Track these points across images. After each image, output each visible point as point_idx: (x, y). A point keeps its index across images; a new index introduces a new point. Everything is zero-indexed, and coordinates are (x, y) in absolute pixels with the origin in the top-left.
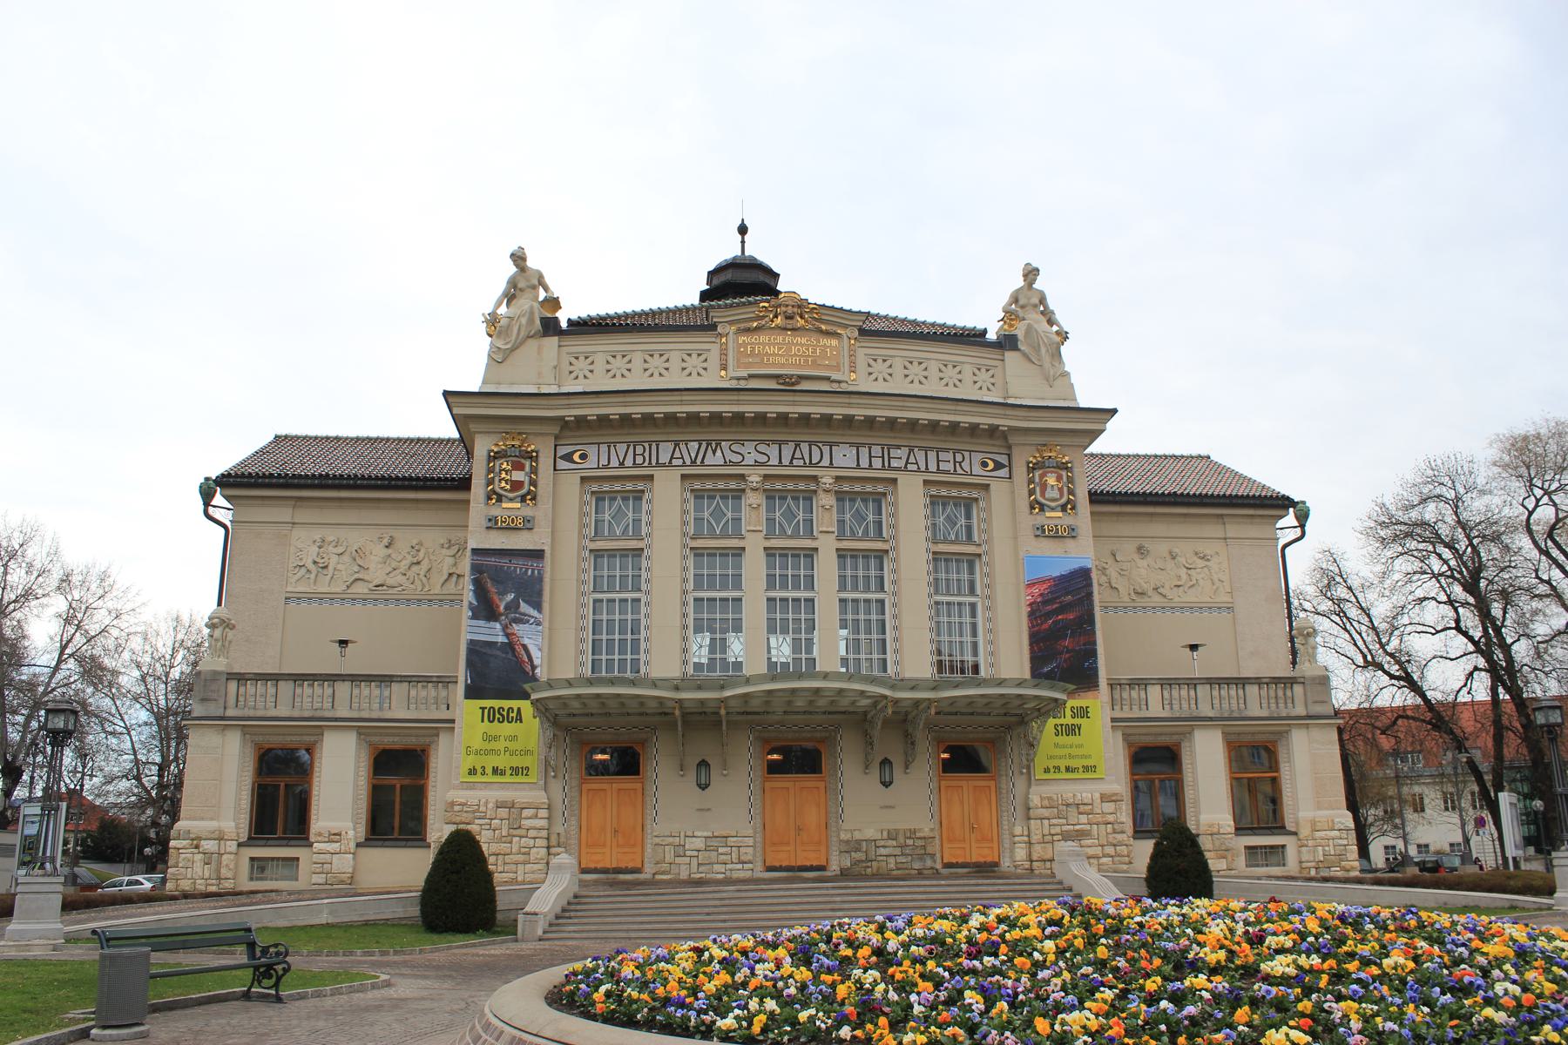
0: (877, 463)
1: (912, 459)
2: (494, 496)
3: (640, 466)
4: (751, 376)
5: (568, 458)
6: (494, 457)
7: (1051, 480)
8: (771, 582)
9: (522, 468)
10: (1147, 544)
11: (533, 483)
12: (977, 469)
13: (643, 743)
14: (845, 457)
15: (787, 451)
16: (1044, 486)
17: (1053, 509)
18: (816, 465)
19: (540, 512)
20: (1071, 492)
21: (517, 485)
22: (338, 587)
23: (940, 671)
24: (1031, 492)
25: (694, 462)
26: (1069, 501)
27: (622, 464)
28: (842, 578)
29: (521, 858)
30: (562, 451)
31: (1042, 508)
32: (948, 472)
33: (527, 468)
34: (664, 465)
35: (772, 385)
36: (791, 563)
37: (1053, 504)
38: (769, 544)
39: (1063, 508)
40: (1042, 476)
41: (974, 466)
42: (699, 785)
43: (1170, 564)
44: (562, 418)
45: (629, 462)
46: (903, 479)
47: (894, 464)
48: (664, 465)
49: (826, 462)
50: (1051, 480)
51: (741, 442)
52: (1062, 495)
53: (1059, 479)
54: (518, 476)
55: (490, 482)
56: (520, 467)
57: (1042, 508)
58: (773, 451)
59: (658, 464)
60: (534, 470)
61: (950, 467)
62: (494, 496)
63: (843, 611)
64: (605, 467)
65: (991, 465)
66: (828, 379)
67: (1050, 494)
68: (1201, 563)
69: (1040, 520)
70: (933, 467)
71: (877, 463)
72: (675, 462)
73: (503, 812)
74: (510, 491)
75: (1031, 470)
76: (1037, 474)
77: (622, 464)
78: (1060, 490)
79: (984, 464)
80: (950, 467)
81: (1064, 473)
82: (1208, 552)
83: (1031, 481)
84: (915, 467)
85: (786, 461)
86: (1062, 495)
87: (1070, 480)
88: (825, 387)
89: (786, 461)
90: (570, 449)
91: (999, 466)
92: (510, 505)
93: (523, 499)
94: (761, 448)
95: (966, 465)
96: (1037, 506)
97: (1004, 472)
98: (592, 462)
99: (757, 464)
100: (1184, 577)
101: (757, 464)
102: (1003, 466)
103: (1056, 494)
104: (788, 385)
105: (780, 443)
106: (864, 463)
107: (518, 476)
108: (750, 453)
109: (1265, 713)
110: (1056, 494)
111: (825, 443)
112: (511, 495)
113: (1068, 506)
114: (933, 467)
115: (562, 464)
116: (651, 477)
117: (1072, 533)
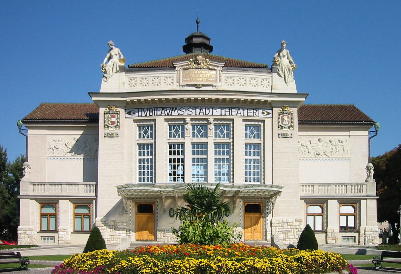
0: (227, 114)
1: (239, 112)
3: (152, 116)
4: (187, 85)
6: (106, 113)
8: (193, 153)
9: (114, 117)
10: (321, 138)
12: (261, 115)
13: (154, 203)
14: (217, 112)
15: (198, 111)
21: (113, 123)
22: (62, 155)
23: (246, 181)
24: (278, 123)
25: (168, 115)
27: (146, 115)
28: (216, 152)
31: (282, 127)
32: (250, 116)
33: (116, 117)
34: (159, 115)
36: (200, 148)
38: (192, 141)
39: (289, 128)
40: (282, 117)
41: (259, 114)
42: (170, 216)
43: (330, 144)
44: (126, 101)
45: (148, 115)
48: (159, 115)
49: (211, 113)
50: (286, 118)
52: (289, 123)
53: (288, 118)
54: (113, 120)
56: (114, 117)
57: (282, 127)
58: (194, 111)
61: (252, 114)
63: (216, 162)
64: (141, 116)
65: (266, 113)
66: (212, 86)
67: (285, 123)
68: (340, 144)
70: (246, 115)
71: (227, 114)
74: (112, 125)
75: (279, 115)
76: (281, 116)
77: (146, 115)
78: (288, 121)
79: (263, 113)
80: (252, 114)
81: (290, 116)
82: (343, 140)
83: (279, 118)
84: (240, 115)
85: (198, 114)
86: (289, 123)
88: (210, 88)
89: (198, 114)
90: (130, 110)
92: (112, 129)
93: (115, 127)
95: (257, 113)
97: (270, 115)
100: (334, 149)
102: (270, 113)
103: (287, 123)
106: (223, 113)
107: (113, 120)
108: (187, 112)
110: (287, 123)
112: (112, 126)
113: (291, 127)
114: (246, 115)
116: (154, 120)
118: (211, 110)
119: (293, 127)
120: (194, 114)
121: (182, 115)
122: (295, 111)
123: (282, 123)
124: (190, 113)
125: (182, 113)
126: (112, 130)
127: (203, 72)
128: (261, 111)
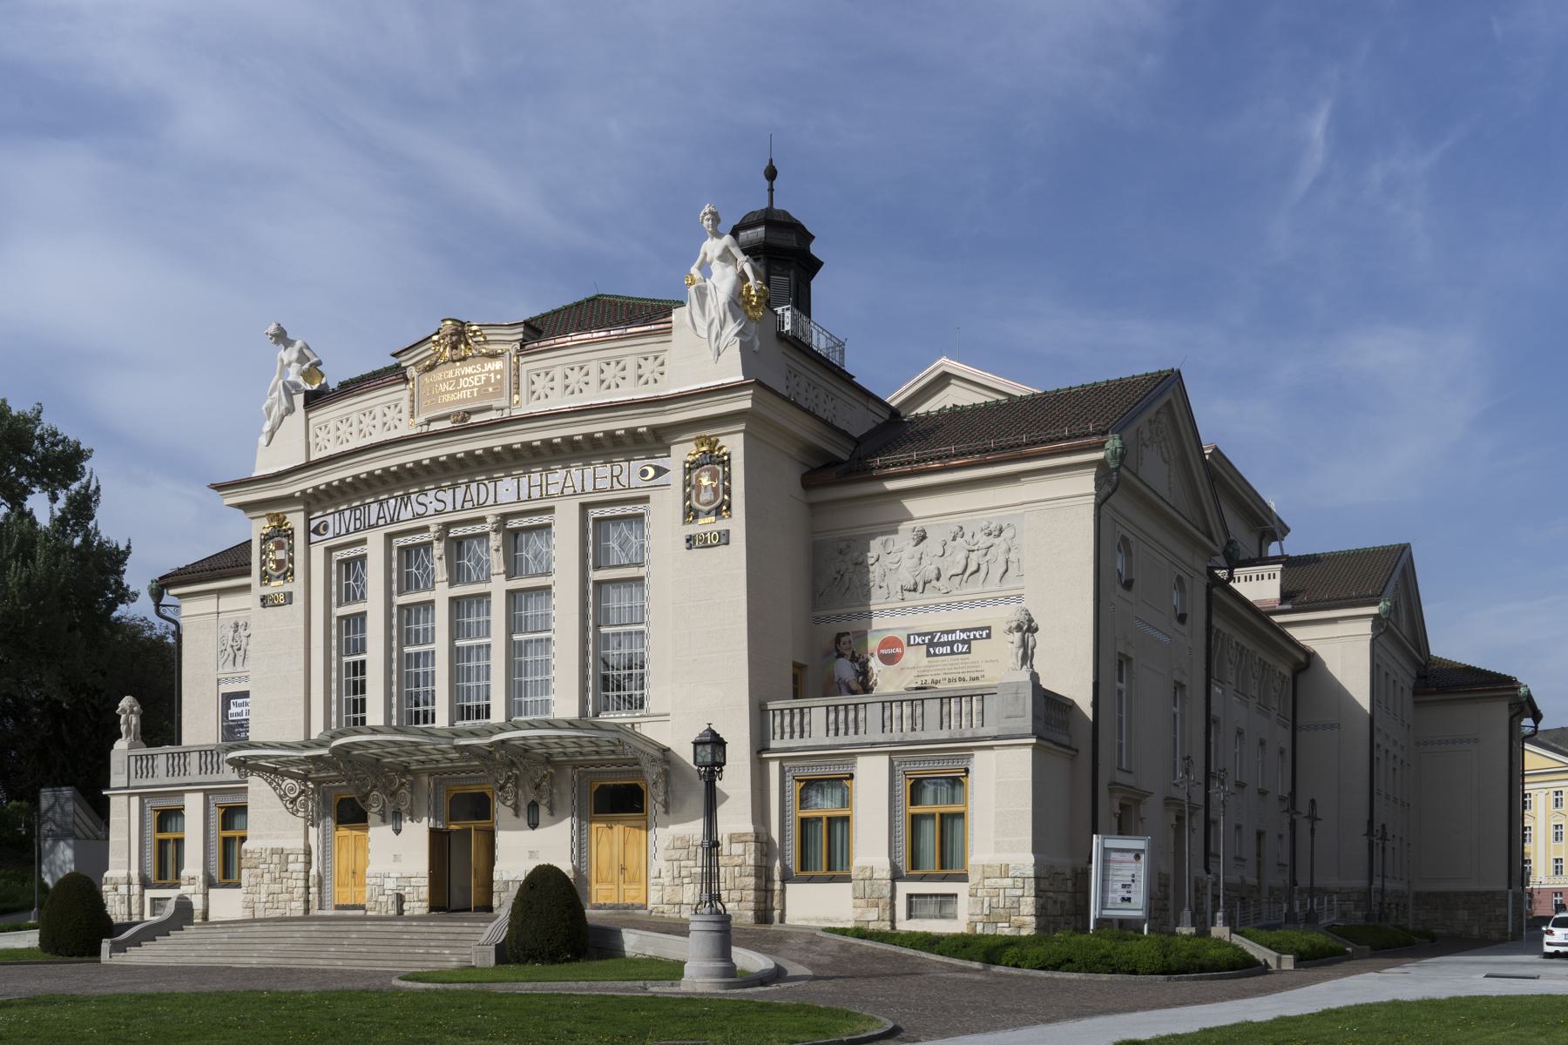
2: (266, 577)
4: (429, 422)
5: (316, 531)
6: (266, 539)
7: (705, 481)
11: (291, 560)
12: (636, 480)
15: (460, 492)
16: (698, 487)
17: (708, 513)
18: (480, 506)
19: (296, 586)
20: (728, 491)
21: (280, 564)
24: (687, 497)
26: (723, 501)
29: (286, 896)
30: (314, 524)
32: (601, 491)
35: (447, 424)
37: (707, 508)
39: (718, 512)
46: (558, 504)
47: (552, 491)
49: (491, 501)
50: (705, 481)
51: (423, 492)
53: (713, 477)
54: (281, 555)
55: (263, 563)
56: (280, 546)
58: (447, 496)
59: (371, 527)
60: (292, 549)
61: (605, 484)
62: (266, 577)
64: (339, 535)
66: (489, 409)
69: (693, 529)
70: (589, 488)
72: (381, 522)
73: (276, 858)
76: (694, 474)
77: (348, 532)
78: (715, 490)
79: (644, 473)
81: (719, 468)
83: (687, 484)
84: (571, 491)
85: (458, 507)
87: (728, 477)
88: (493, 416)
89: (458, 507)
91: (660, 471)
94: (441, 495)
96: (691, 514)
97: (662, 480)
98: (330, 534)
99: (438, 512)
101: (438, 512)
104: (463, 425)
105: (454, 486)
107: (281, 555)
109: (944, 734)
111: (490, 479)
114: (589, 488)
115: (314, 537)
117: (724, 538)
118: (491, 486)
119: (729, 508)
120: (449, 508)
121: (421, 516)
122: (733, 444)
123: (698, 500)
124: (440, 506)
125: (421, 510)
126: (277, 587)
127: (469, 370)
128: (636, 465)
